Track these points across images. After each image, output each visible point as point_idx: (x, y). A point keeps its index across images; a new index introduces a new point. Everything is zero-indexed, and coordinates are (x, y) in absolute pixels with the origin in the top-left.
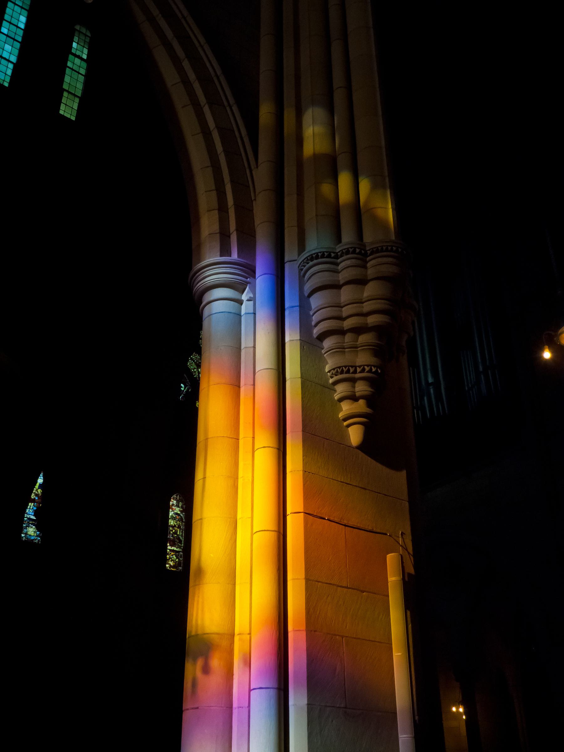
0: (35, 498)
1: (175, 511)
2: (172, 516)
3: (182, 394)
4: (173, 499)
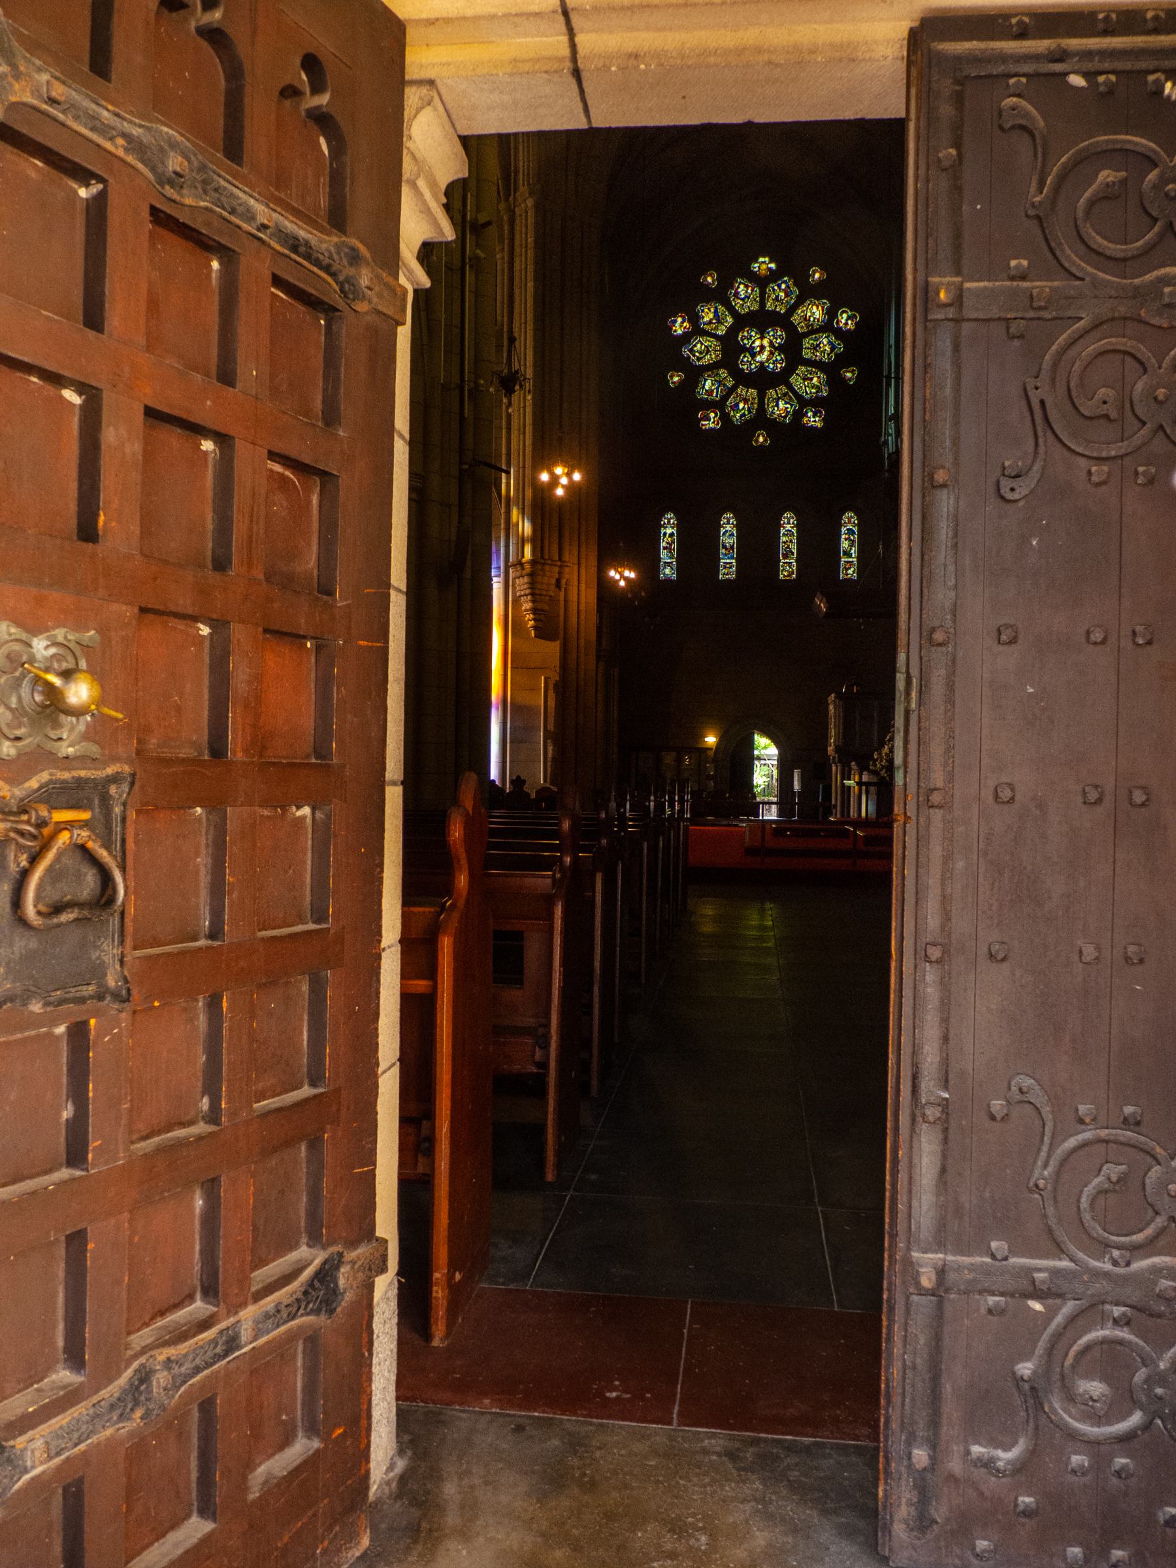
2: (784, 534)
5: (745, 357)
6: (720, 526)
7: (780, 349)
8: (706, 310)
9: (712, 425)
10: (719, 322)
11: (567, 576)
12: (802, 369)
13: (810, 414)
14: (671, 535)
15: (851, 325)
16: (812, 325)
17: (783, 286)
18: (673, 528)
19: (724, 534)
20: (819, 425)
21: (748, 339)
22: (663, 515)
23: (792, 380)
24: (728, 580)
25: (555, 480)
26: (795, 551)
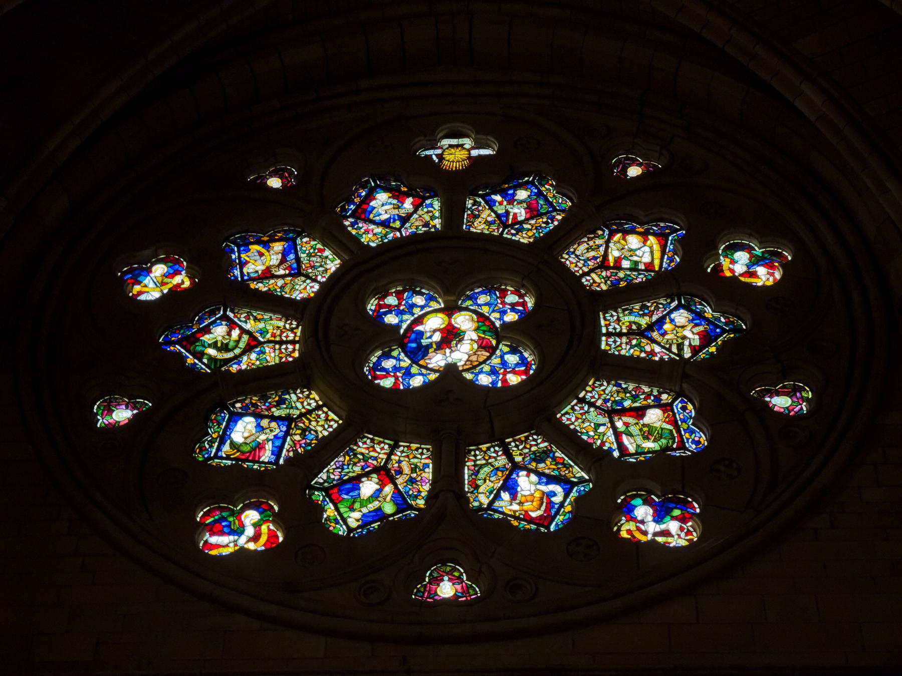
3: (557, 513)
5: (387, 356)
13: (643, 511)
15: (764, 277)
21: (400, 313)
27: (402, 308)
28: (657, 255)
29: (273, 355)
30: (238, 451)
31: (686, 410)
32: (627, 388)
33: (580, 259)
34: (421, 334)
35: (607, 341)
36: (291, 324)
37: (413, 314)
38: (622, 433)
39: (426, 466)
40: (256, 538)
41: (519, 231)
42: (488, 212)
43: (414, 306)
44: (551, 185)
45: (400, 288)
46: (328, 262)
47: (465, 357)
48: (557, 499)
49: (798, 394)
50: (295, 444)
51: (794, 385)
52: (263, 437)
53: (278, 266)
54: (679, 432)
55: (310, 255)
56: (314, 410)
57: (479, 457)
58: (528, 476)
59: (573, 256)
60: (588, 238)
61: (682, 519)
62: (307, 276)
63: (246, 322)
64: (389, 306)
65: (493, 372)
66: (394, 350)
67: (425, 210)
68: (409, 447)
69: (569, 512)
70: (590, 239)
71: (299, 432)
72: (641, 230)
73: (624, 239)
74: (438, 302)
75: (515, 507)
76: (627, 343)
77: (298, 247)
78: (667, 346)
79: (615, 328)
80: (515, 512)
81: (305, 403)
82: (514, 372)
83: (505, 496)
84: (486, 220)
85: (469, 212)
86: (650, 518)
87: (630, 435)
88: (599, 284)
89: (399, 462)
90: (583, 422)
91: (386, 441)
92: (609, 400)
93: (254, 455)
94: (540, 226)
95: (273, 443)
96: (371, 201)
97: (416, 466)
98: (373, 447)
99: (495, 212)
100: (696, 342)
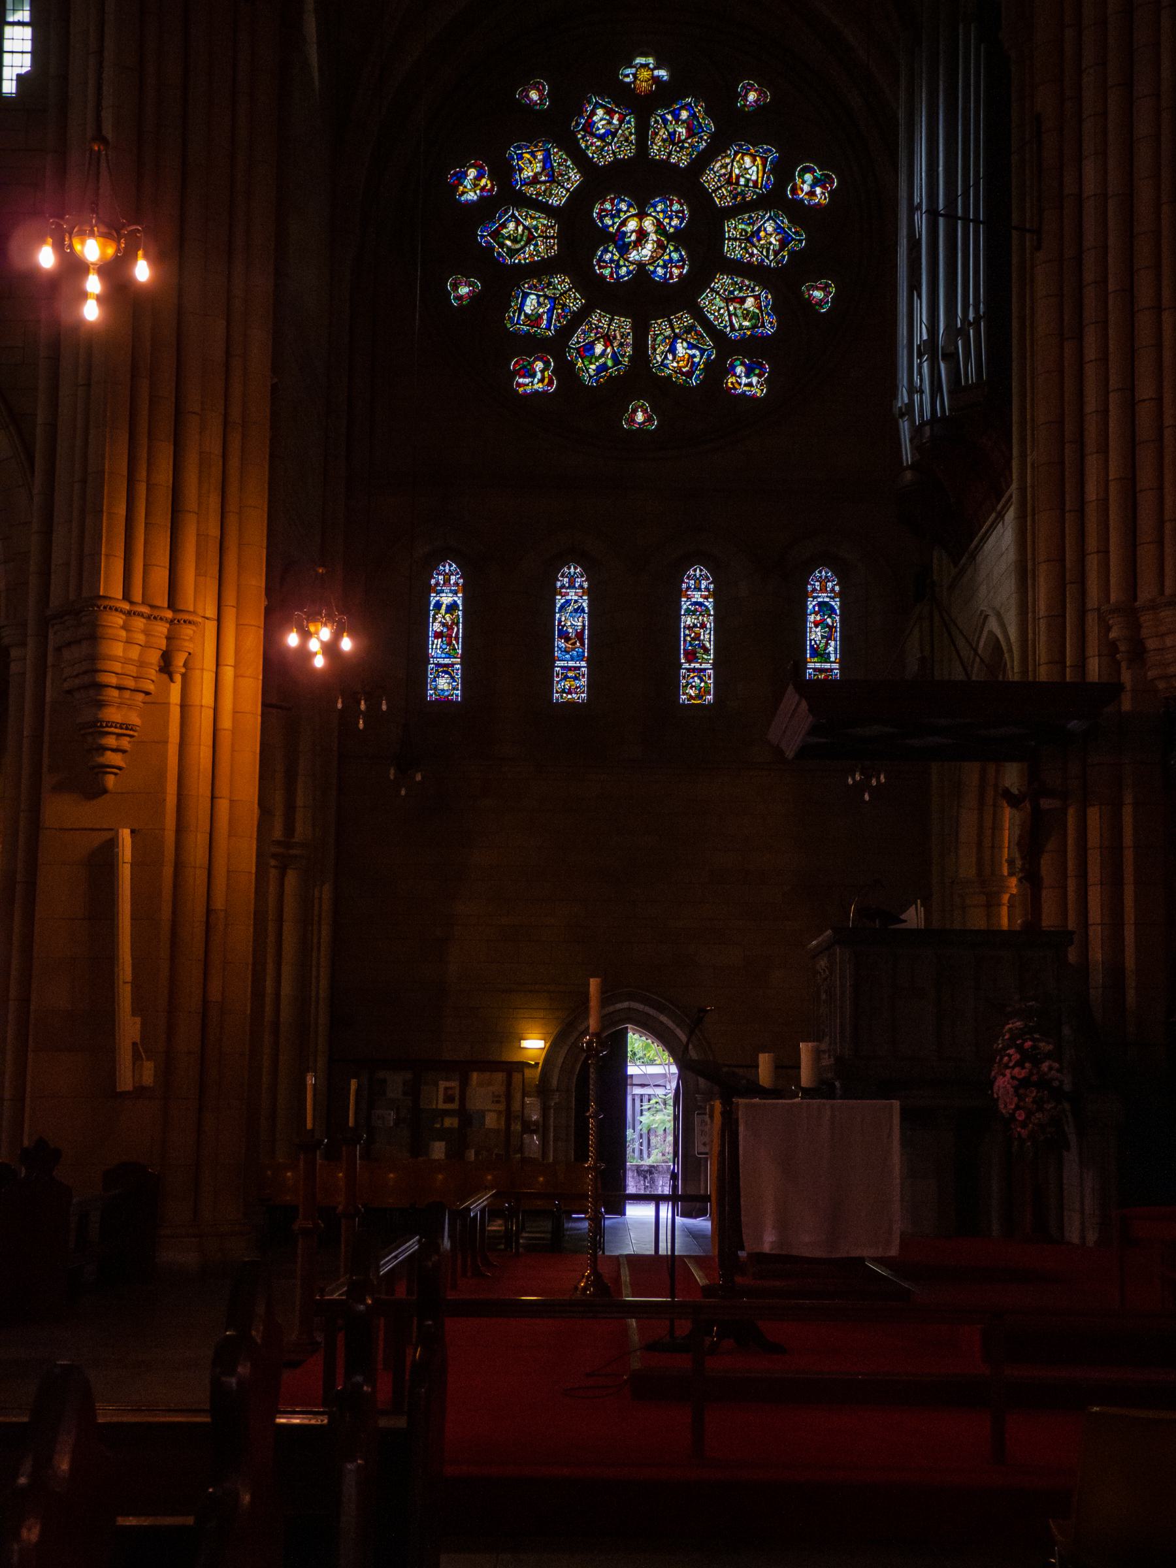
0: (442, 631)
1: (693, 600)
2: (688, 610)
3: (696, 369)
4: (688, 578)
5: (606, 251)
6: (554, 592)
7: (678, 238)
8: (528, 156)
9: (539, 387)
10: (552, 179)
11: (189, 646)
12: (723, 281)
13: (739, 370)
14: (452, 608)
15: (821, 196)
16: (742, 194)
17: (684, 115)
18: (455, 593)
19: (562, 607)
20: (758, 391)
21: (613, 217)
22: (436, 568)
23: (704, 301)
24: (569, 704)
25: (74, 268)
26: (710, 646)
27: (614, 212)
28: (760, 175)
29: (542, 247)
30: (529, 320)
31: (766, 296)
32: (737, 281)
33: (716, 175)
34: (625, 233)
35: (728, 244)
36: (551, 222)
37: (620, 218)
38: (733, 314)
39: (629, 334)
40: (541, 381)
41: (682, 148)
42: (663, 130)
43: (619, 211)
44: (702, 106)
45: (612, 196)
46: (570, 171)
47: (650, 253)
48: (696, 360)
49: (828, 289)
50: (559, 316)
51: (826, 282)
52: (541, 310)
53: (541, 173)
54: (762, 315)
55: (559, 165)
56: (568, 291)
57: (657, 329)
58: (682, 343)
59: (712, 172)
60: (722, 156)
61: (759, 376)
62: (559, 184)
63: (525, 220)
64: (605, 210)
65: (664, 267)
66: (610, 246)
67: (626, 126)
68: (619, 320)
69: (702, 369)
70: (723, 158)
71: (560, 307)
72: (752, 151)
73: (743, 160)
74: (634, 209)
75: (675, 364)
76: (740, 246)
77: (552, 156)
78: (761, 250)
79: (733, 234)
80: (675, 367)
81: (563, 286)
82: (677, 267)
83: (670, 357)
84: (663, 138)
85: (652, 130)
86: (743, 375)
87: (736, 316)
88: (727, 196)
89: (615, 330)
90: (712, 305)
91: (608, 316)
92: (727, 289)
93: (538, 324)
94: (694, 145)
95: (547, 315)
96: (593, 116)
97: (624, 334)
98: (600, 319)
99: (668, 131)
100: (777, 248)
